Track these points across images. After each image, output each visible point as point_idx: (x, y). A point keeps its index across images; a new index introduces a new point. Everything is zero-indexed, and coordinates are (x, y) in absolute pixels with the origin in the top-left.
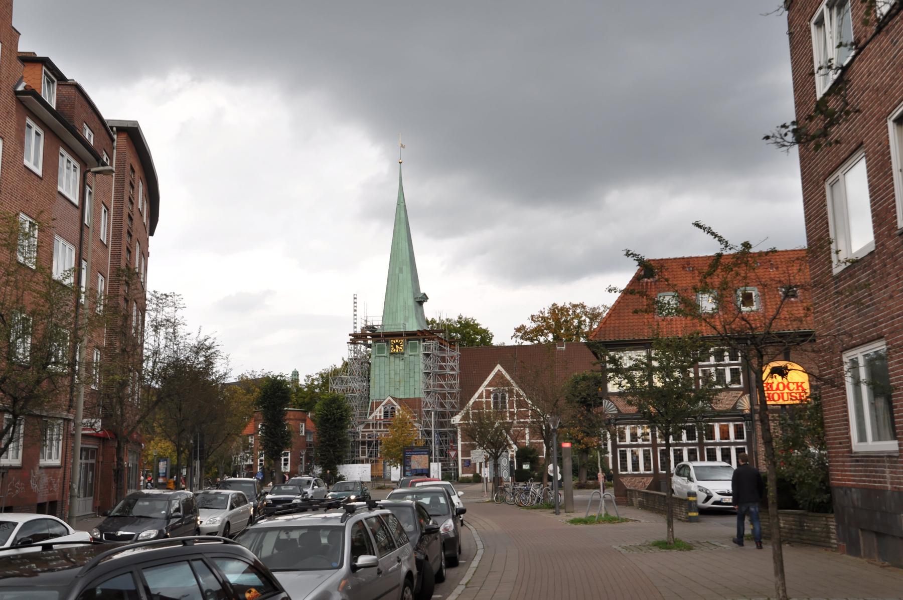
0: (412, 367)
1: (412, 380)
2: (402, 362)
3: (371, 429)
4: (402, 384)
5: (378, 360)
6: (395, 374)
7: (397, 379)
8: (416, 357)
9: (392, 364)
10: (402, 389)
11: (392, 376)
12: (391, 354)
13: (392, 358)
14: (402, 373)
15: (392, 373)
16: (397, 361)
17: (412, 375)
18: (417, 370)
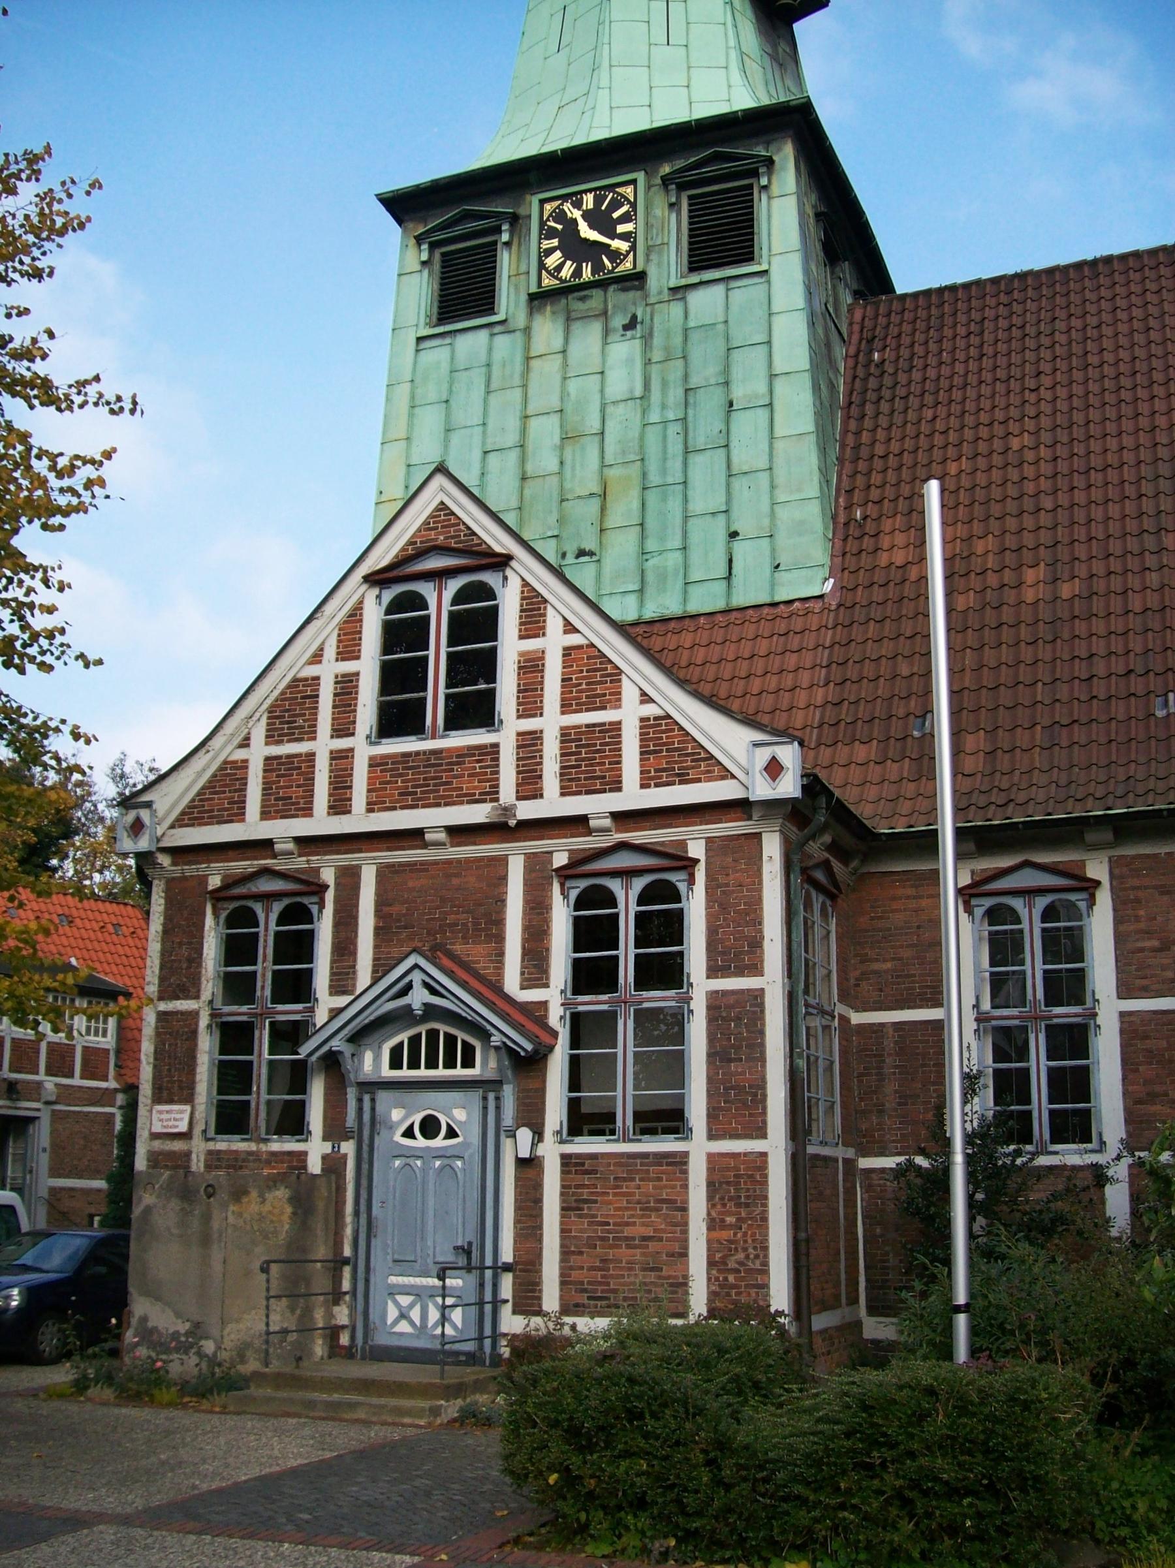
0: (705, 371)
1: (705, 471)
2: (625, 350)
3: (252, 827)
4: (624, 508)
5: (437, 355)
6: (568, 438)
7: (585, 479)
8: (746, 294)
9: (546, 371)
10: (621, 549)
11: (545, 460)
12: (539, 299)
13: (547, 330)
14: (622, 424)
15: (545, 431)
16: (588, 337)
17: (707, 423)
18: (748, 385)
